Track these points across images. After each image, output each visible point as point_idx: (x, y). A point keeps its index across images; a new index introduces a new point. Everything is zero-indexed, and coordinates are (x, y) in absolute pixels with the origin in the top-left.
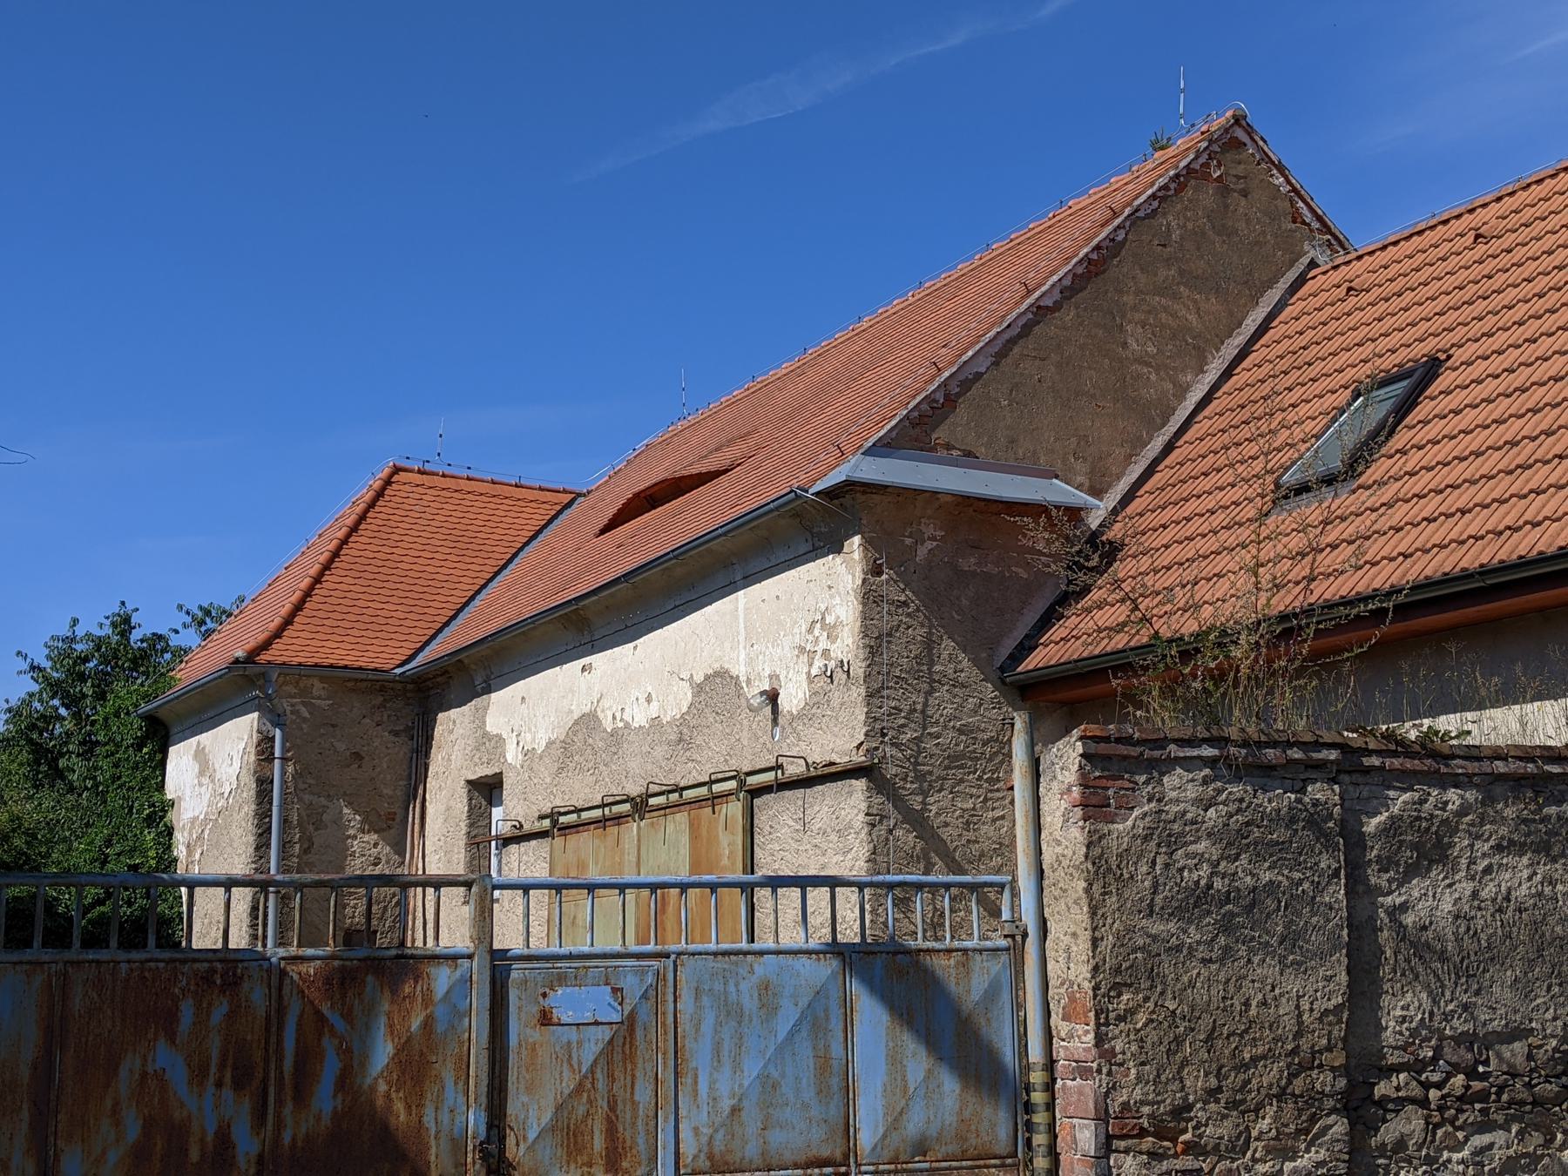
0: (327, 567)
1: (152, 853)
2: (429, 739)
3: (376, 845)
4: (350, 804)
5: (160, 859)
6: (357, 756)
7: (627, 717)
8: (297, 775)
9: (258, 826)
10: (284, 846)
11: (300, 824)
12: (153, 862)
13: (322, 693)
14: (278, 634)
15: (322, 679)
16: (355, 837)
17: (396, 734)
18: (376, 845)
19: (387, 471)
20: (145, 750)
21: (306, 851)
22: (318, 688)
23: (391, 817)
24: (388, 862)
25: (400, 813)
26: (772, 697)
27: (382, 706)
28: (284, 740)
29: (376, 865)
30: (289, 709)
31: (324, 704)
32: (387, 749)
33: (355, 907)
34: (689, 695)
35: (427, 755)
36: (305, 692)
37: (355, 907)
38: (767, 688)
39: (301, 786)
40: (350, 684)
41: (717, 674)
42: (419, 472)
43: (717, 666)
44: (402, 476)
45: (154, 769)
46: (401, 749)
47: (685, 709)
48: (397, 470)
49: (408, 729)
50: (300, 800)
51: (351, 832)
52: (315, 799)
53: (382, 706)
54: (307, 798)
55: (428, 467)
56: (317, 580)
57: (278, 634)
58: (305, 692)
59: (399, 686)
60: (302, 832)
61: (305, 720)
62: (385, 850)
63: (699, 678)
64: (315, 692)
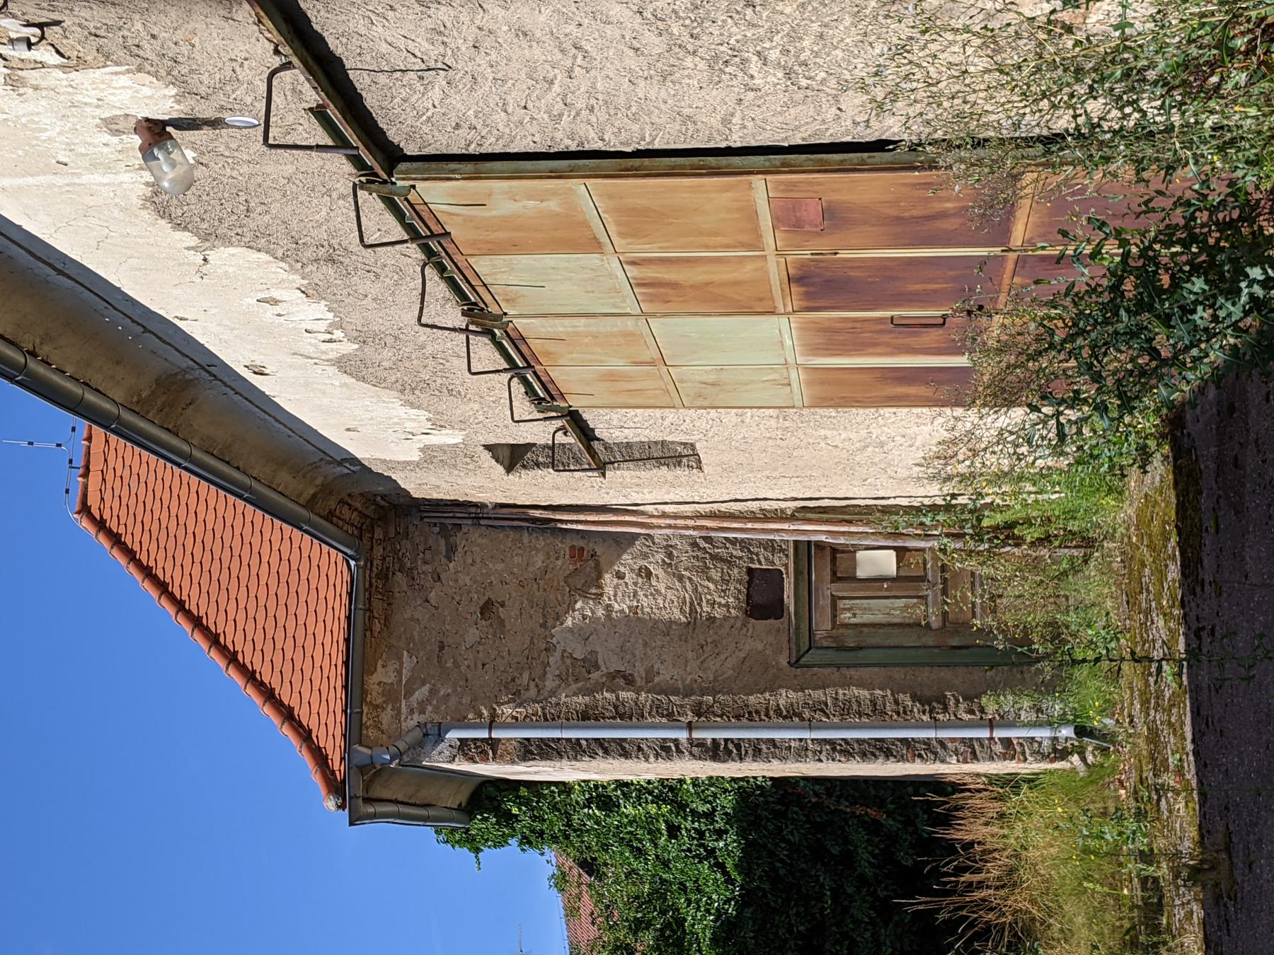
0: (214, 640)
1: (653, 809)
2: (455, 504)
3: (620, 576)
4: (559, 618)
5: (658, 799)
6: (487, 608)
7: (322, 326)
8: (517, 698)
9: (593, 755)
10: (624, 715)
11: (589, 692)
12: (665, 809)
13: (391, 668)
14: (305, 735)
15: (368, 668)
16: (608, 608)
17: (451, 551)
18: (620, 576)
19: (85, 523)
20: (515, 811)
21: (629, 681)
22: (382, 675)
23: (577, 553)
24: (645, 556)
25: (569, 542)
26: (156, 133)
27: (409, 573)
28: (462, 723)
29: (649, 574)
30: (417, 718)
31: (408, 662)
32: (475, 566)
33: (713, 604)
34: (231, 250)
35: (483, 506)
36: (391, 695)
37: (713, 604)
38: (137, 140)
39: (533, 692)
40: (377, 626)
41: (163, 212)
42: (86, 474)
43: (147, 215)
44: (93, 501)
45: (540, 796)
46: (474, 541)
47: (264, 257)
48: (85, 509)
49: (445, 532)
50: (553, 693)
51: (600, 612)
52: (552, 671)
53: (409, 573)
54: (550, 684)
55: (80, 462)
56: (232, 658)
57: (305, 735)
58: (391, 695)
59: (378, 551)
60: (599, 687)
61: (433, 692)
62: (628, 561)
63: (189, 239)
64: (391, 678)
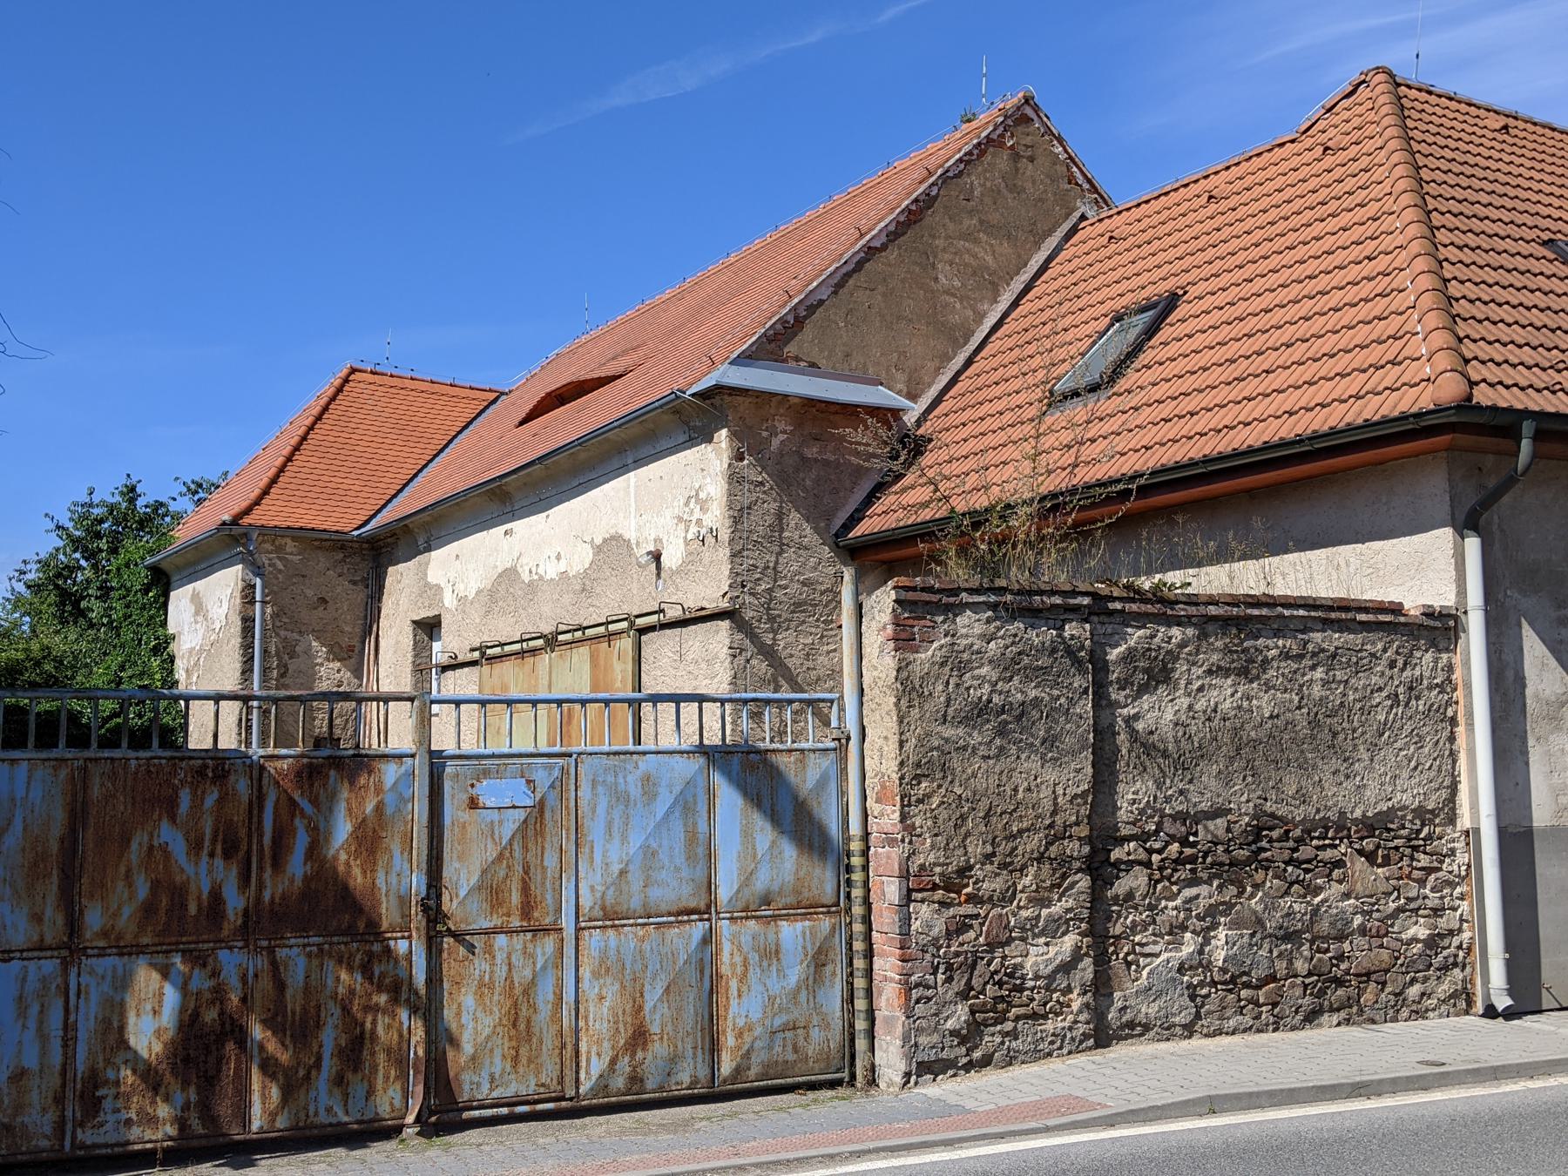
0: (297, 449)
2: (381, 588)
6: (323, 601)
7: (541, 571)
8: (275, 616)
9: (244, 655)
10: (265, 671)
11: (277, 654)
14: (257, 502)
15: (294, 539)
17: (355, 583)
21: (283, 675)
22: (290, 545)
23: (351, 649)
28: (264, 587)
32: (347, 596)
35: (380, 600)
36: (279, 549)
41: (612, 538)
43: (612, 531)
48: (353, 371)
49: (364, 580)
50: (277, 635)
51: (319, 661)
52: (289, 634)
54: (282, 633)
55: (378, 369)
56: (289, 459)
57: (257, 502)
58: (279, 549)
61: (280, 571)
63: (598, 541)
64: (288, 549)
